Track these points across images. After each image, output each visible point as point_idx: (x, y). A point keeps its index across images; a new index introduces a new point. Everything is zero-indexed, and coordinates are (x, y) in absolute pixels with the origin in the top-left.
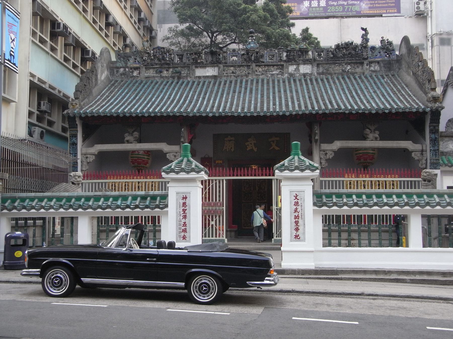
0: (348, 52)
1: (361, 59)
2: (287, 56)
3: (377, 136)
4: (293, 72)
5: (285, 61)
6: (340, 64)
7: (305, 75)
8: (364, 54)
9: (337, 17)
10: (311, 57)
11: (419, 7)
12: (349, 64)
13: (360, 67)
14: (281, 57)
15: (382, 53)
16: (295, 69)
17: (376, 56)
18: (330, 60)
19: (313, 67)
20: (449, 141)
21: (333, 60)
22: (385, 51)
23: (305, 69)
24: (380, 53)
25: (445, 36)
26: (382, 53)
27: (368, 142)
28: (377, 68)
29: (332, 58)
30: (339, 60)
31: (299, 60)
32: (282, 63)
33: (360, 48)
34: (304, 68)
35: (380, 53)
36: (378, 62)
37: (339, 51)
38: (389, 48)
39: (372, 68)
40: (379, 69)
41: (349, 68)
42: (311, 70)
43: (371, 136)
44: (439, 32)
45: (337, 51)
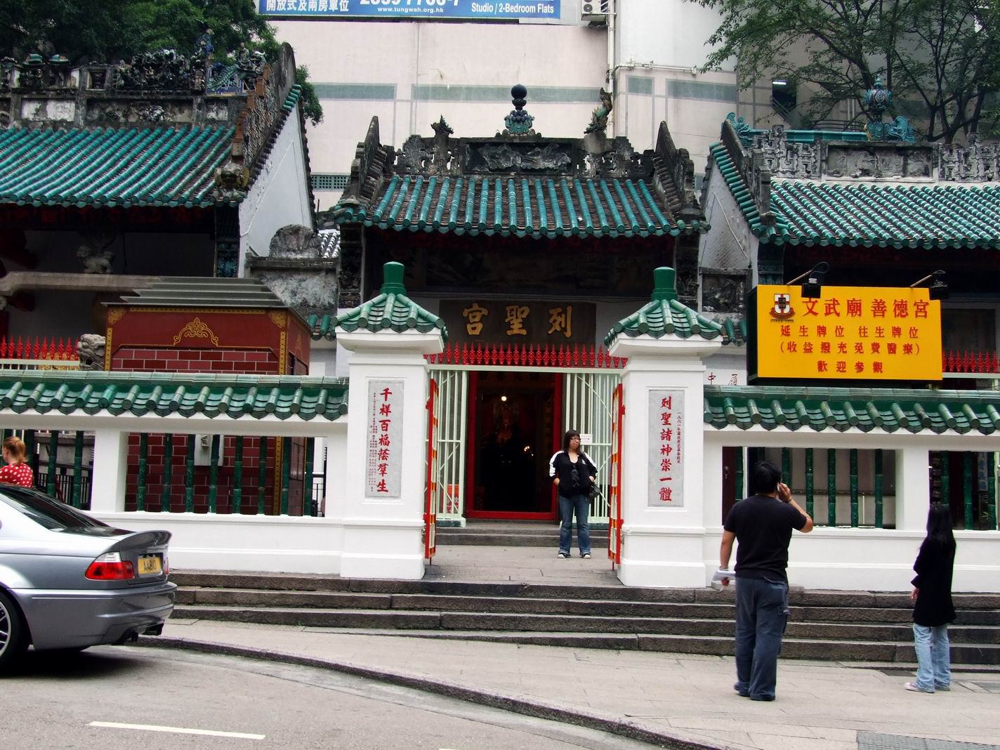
0: (158, 77)
1: (189, 92)
2: (20, 80)
3: (105, 262)
4: (31, 117)
5: (15, 91)
6: (142, 104)
7: (56, 124)
8: (198, 81)
9: (410, 20)
10: (77, 85)
11: (591, 8)
12: (163, 103)
13: (186, 112)
14: (6, 81)
15: (237, 80)
16: (37, 110)
17: (224, 86)
18: (119, 93)
19: (77, 108)
20: (274, 280)
21: (125, 93)
22: (243, 75)
23: (61, 111)
24: (232, 79)
25: (638, 74)
26: (237, 80)
27: (86, 276)
28: (223, 115)
29: (121, 87)
30: (139, 94)
31: (49, 90)
32: (8, 96)
33: (188, 67)
34: (57, 108)
35: (232, 79)
36: (225, 101)
37: (142, 71)
38: (254, 70)
39: (212, 115)
40: (226, 118)
41: (158, 112)
42: (73, 114)
43: (93, 263)
44: (628, 63)
45: (137, 71)
